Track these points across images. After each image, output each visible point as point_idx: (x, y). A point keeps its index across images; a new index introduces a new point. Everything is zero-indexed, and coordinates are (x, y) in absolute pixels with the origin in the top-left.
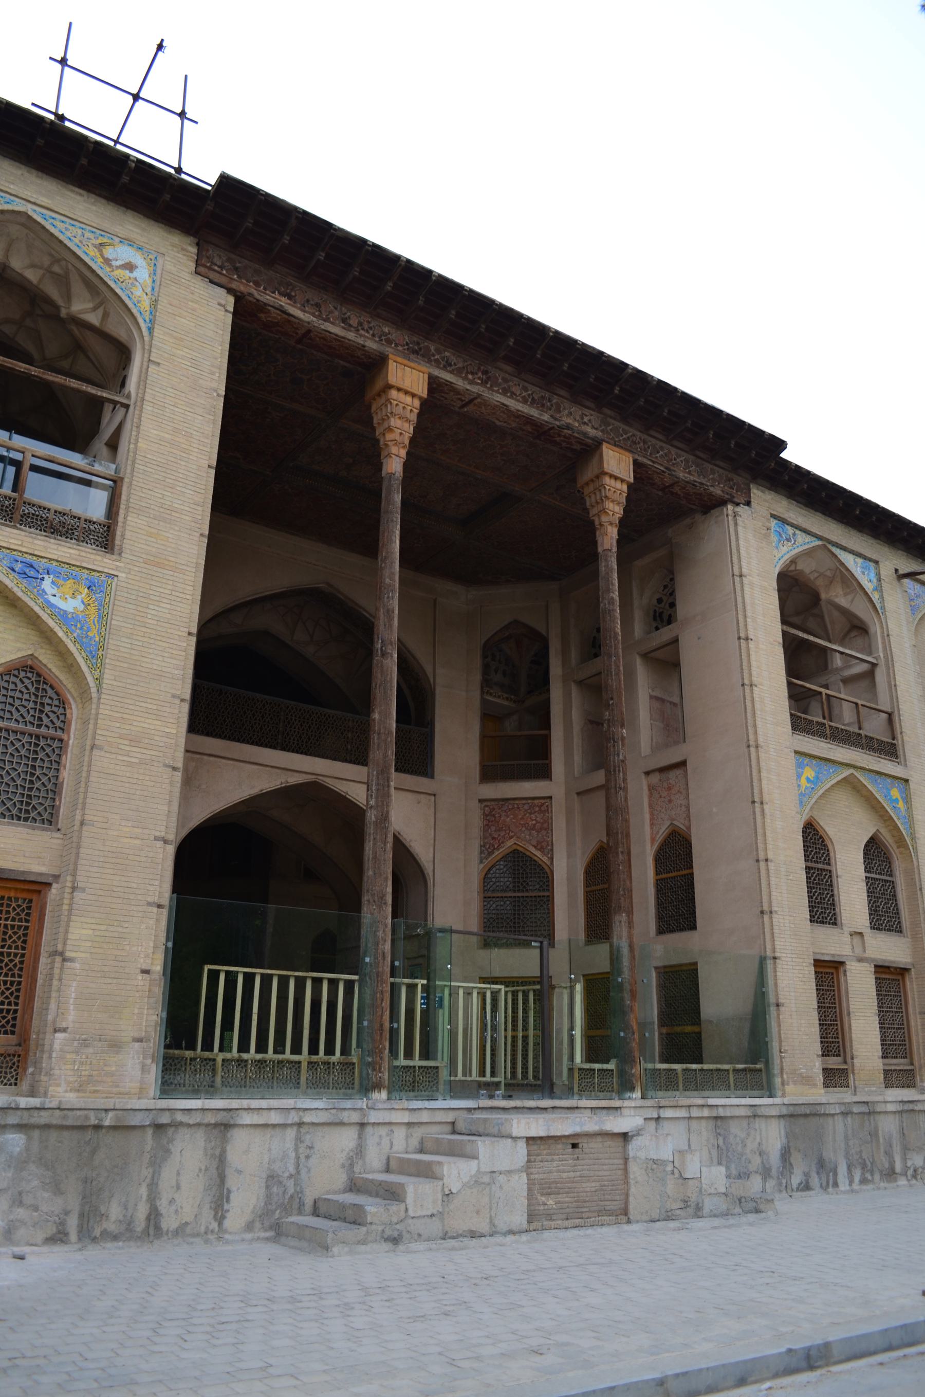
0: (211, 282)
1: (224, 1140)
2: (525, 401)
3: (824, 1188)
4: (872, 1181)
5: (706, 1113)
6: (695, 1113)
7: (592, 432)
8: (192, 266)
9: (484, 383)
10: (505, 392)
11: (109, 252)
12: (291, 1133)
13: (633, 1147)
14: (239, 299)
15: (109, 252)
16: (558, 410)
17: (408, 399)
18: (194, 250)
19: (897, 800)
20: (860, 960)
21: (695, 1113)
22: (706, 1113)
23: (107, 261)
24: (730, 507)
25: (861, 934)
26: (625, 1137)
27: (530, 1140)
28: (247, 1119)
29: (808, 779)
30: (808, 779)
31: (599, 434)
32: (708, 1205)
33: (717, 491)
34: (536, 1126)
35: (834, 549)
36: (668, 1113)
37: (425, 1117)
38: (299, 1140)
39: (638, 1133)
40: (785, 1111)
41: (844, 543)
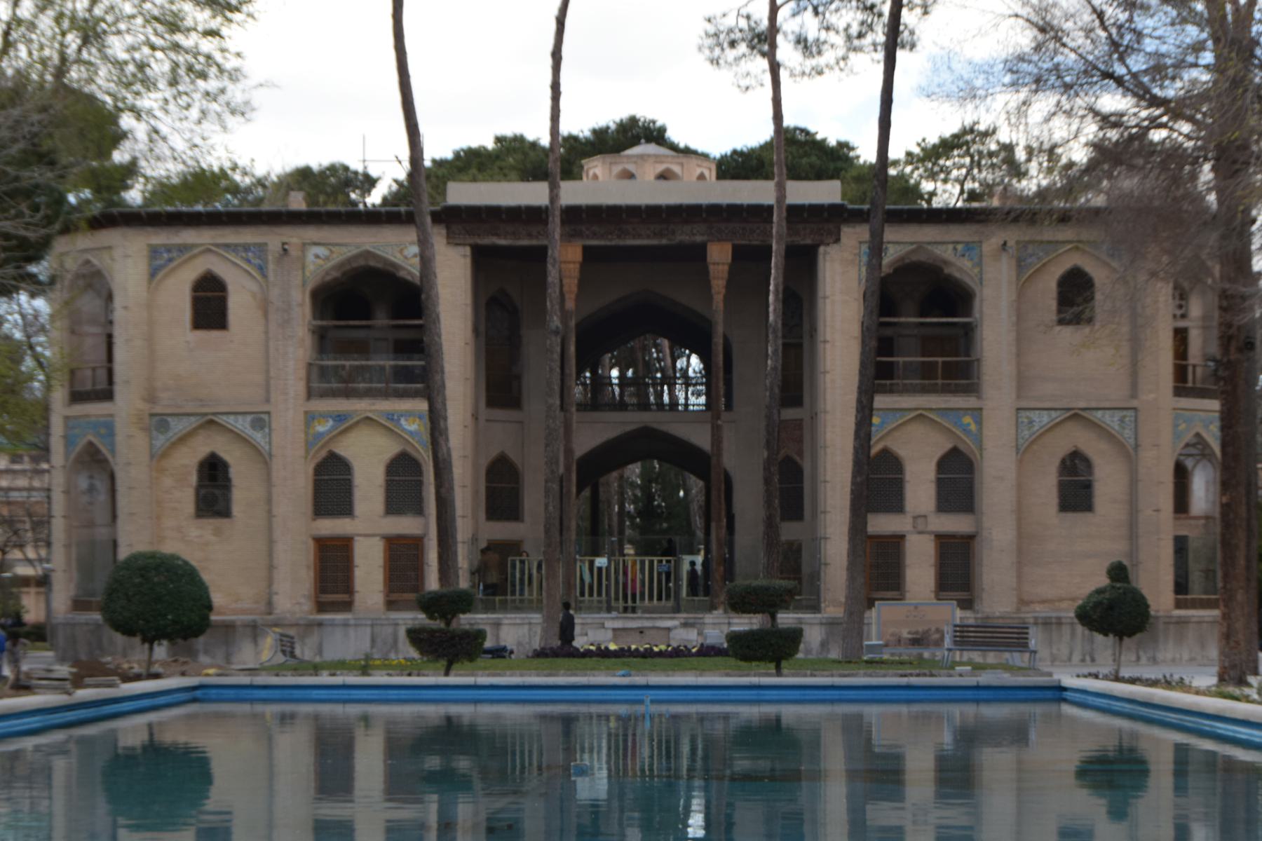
0: (457, 244)
1: (498, 630)
2: (648, 237)
7: (699, 239)
8: (445, 241)
9: (619, 237)
10: (634, 238)
11: (406, 252)
12: (526, 627)
13: (672, 634)
15: (406, 252)
16: (673, 233)
17: (572, 266)
18: (444, 232)
19: (969, 424)
23: (406, 257)
24: (822, 249)
25: (925, 516)
26: (669, 629)
27: (614, 630)
28: (506, 621)
31: (705, 238)
33: (808, 241)
34: (619, 624)
35: (929, 247)
37: (589, 621)
38: (530, 630)
39: (675, 628)
41: (938, 239)
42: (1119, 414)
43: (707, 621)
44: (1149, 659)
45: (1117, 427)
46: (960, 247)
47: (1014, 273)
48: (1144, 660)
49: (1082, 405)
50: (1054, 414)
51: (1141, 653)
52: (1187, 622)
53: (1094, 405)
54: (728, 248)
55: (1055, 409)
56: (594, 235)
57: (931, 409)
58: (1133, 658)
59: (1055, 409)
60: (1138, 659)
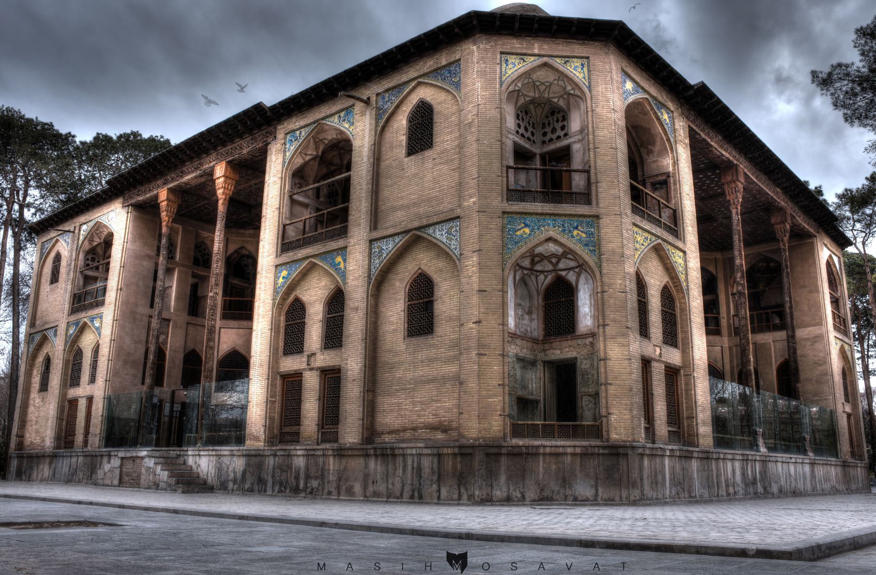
2: (193, 172)
3: (259, 492)
4: (284, 492)
5: (214, 453)
6: (210, 453)
14: (132, 205)
20: (311, 369)
21: (210, 453)
22: (214, 453)
29: (284, 278)
30: (284, 278)
32: (162, 485)
36: (202, 453)
40: (244, 453)
42: (446, 227)
43: (190, 453)
44: (469, 499)
45: (445, 241)
46: (342, 114)
47: (373, 122)
48: (465, 497)
49: (416, 224)
50: (397, 239)
51: (463, 490)
52: (537, 454)
53: (425, 222)
54: (224, 164)
55: (398, 234)
56: (173, 180)
57: (316, 255)
58: (456, 496)
59: (398, 234)
60: (459, 499)
